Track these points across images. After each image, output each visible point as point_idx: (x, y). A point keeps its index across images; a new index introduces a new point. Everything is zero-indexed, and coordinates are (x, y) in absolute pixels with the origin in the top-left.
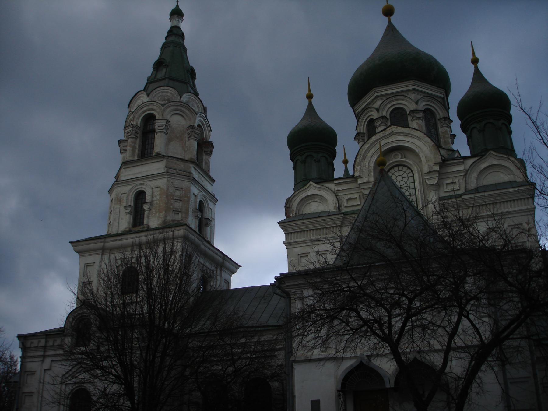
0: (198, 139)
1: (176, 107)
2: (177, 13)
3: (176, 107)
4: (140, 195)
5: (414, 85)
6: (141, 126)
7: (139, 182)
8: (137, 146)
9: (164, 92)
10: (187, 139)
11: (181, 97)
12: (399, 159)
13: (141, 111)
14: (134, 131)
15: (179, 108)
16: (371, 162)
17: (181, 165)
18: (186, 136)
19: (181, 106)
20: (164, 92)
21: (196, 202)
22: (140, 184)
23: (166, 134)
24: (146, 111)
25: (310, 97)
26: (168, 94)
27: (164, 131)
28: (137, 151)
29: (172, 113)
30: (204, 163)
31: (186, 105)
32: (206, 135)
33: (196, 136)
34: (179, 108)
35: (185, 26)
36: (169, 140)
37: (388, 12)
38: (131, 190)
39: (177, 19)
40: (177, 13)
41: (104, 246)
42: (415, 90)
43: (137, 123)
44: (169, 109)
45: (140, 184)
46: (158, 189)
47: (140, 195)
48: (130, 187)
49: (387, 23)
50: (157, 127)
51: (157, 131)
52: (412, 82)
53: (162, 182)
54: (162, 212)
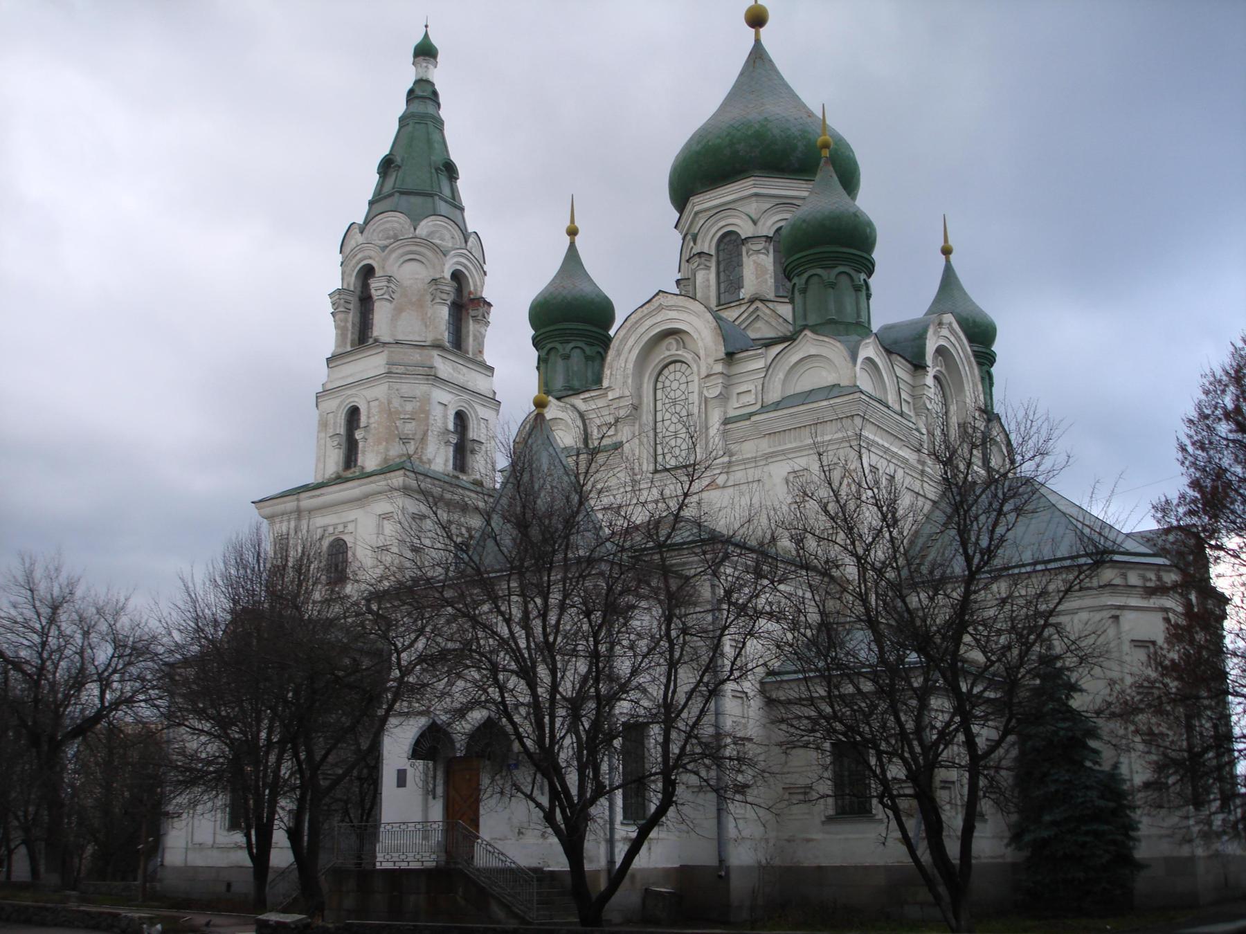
0: (448, 302)
1: (408, 248)
2: (425, 51)
3: (408, 248)
4: (354, 413)
5: (755, 186)
6: (355, 288)
7: (349, 392)
8: (350, 325)
9: (388, 222)
10: (429, 303)
11: (415, 229)
12: (673, 352)
13: (354, 261)
14: (342, 301)
15: (414, 248)
16: (629, 360)
17: (416, 356)
18: (429, 298)
19: (417, 244)
20: (388, 222)
21: (445, 417)
22: (351, 396)
23: (391, 302)
24: (361, 260)
25: (573, 232)
26: (396, 225)
27: (386, 296)
28: (349, 335)
29: (402, 260)
30: (471, 339)
31: (427, 242)
32: (475, 285)
33: (445, 296)
34: (414, 248)
35: (439, 76)
36: (399, 310)
37: (757, 19)
38: (339, 406)
39: (425, 64)
40: (425, 51)
41: (298, 507)
42: (756, 195)
43: (348, 285)
44: (394, 255)
45: (351, 396)
46: (377, 402)
47: (354, 413)
48: (337, 401)
49: (751, 43)
50: (373, 291)
51: (375, 298)
52: (749, 182)
53: (380, 391)
54: (380, 444)
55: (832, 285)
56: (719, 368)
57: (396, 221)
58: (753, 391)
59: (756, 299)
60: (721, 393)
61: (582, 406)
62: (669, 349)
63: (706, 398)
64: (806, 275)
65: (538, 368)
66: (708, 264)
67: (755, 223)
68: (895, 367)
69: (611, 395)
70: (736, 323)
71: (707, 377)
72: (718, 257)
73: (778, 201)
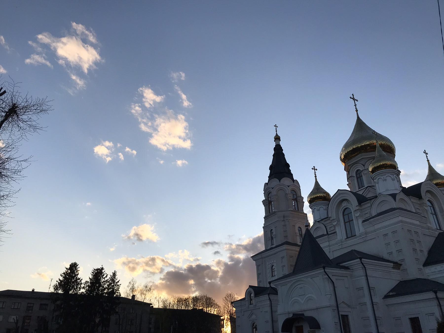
55: (386, 180)
56: (358, 208)
57: (276, 182)
58: (369, 213)
59: (368, 186)
60: (360, 214)
61: (325, 223)
62: (344, 204)
63: (356, 216)
64: (377, 178)
65: (312, 214)
66: (354, 179)
67: (364, 166)
68: (411, 199)
69: (331, 219)
70: (363, 195)
71: (355, 211)
72: (357, 177)
73: (369, 159)
